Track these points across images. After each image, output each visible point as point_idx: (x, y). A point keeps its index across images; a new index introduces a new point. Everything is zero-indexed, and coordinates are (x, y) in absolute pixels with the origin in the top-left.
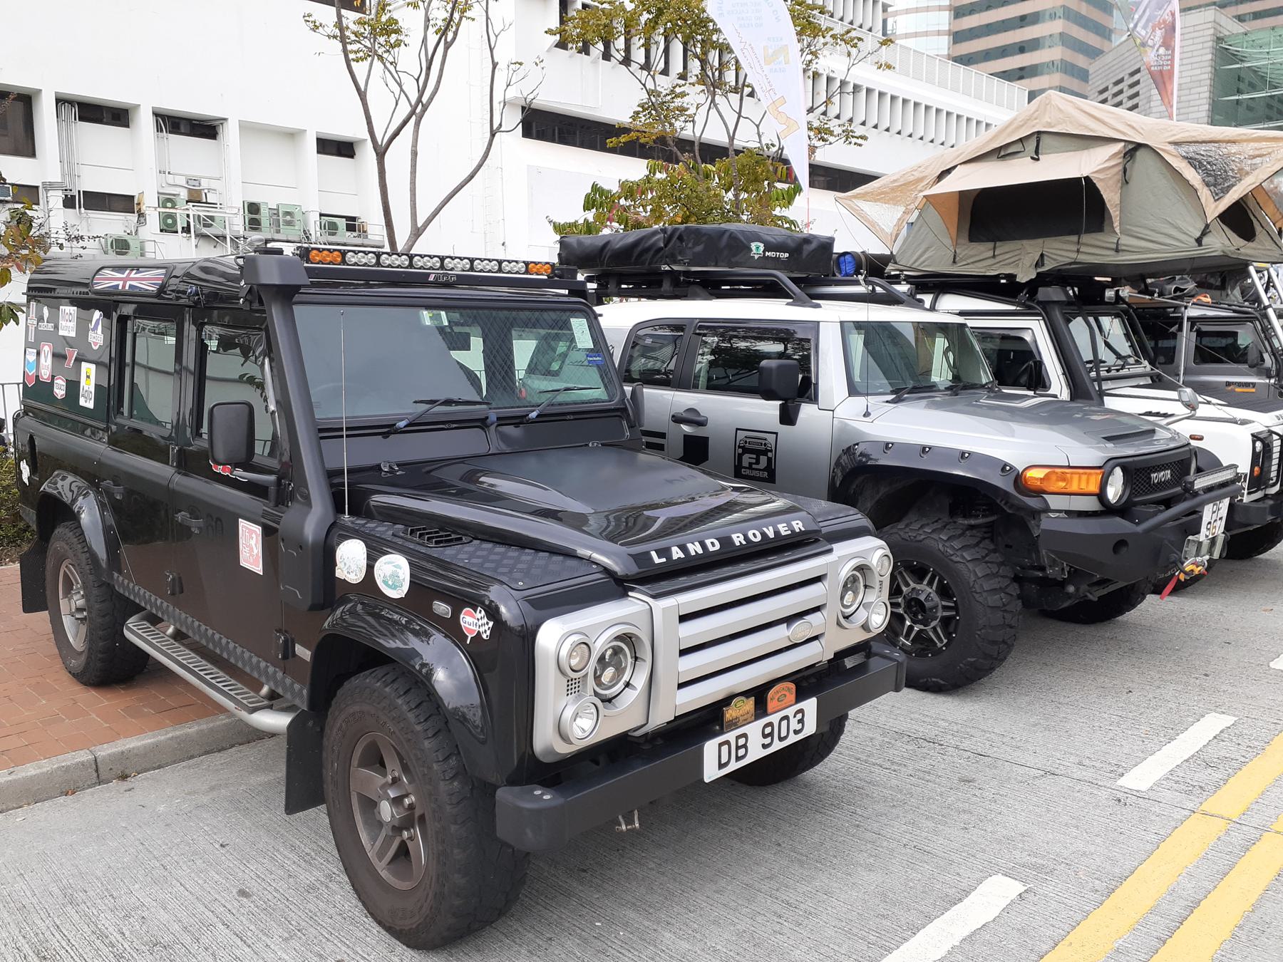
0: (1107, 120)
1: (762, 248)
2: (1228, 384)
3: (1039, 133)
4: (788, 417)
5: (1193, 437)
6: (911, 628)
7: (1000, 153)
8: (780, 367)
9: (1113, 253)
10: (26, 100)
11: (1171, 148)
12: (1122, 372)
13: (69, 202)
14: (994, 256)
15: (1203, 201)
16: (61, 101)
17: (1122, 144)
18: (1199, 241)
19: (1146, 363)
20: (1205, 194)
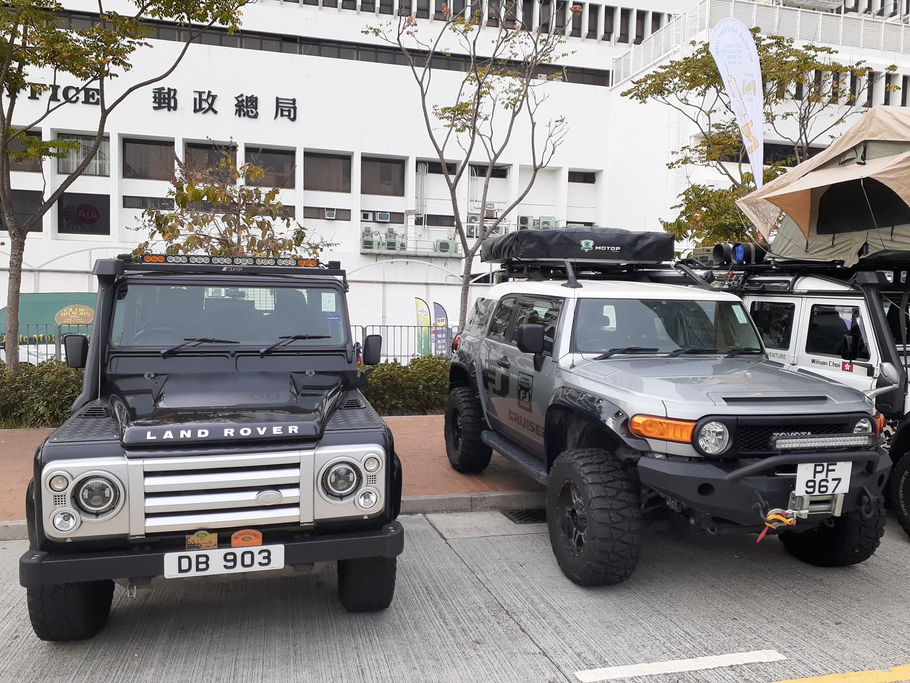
1: (591, 243)
3: (866, 142)
7: (840, 160)
10: (401, 163)
13: (418, 222)
14: (833, 246)
16: (419, 162)
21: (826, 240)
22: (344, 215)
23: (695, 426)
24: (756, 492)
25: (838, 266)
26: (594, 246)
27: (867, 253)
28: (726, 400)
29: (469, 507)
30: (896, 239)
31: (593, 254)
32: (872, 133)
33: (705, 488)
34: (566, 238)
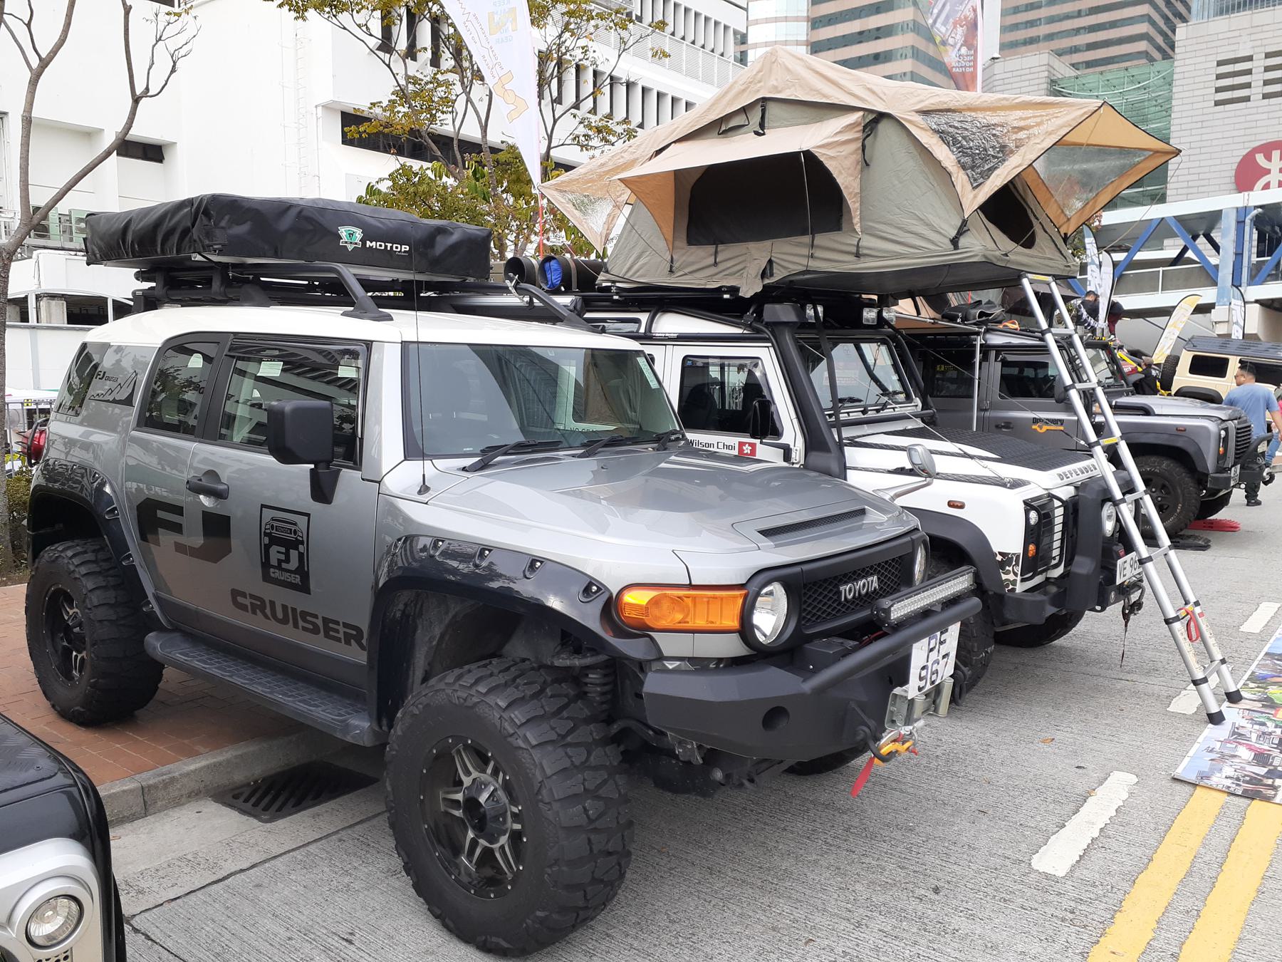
0: (842, 82)
1: (358, 234)
2: (1036, 421)
3: (764, 100)
4: (322, 490)
5: (951, 504)
6: (474, 843)
7: (720, 127)
8: (297, 411)
9: (852, 258)
11: (918, 118)
12: (883, 414)
14: (716, 264)
15: (959, 188)
17: (861, 113)
18: (955, 242)
19: (918, 401)
20: (961, 179)
21: (702, 254)
23: (746, 596)
24: (853, 705)
25: (726, 296)
26: (363, 241)
27: (772, 275)
30: (818, 253)
31: (362, 257)
32: (776, 87)
33: (774, 715)
34: (309, 220)
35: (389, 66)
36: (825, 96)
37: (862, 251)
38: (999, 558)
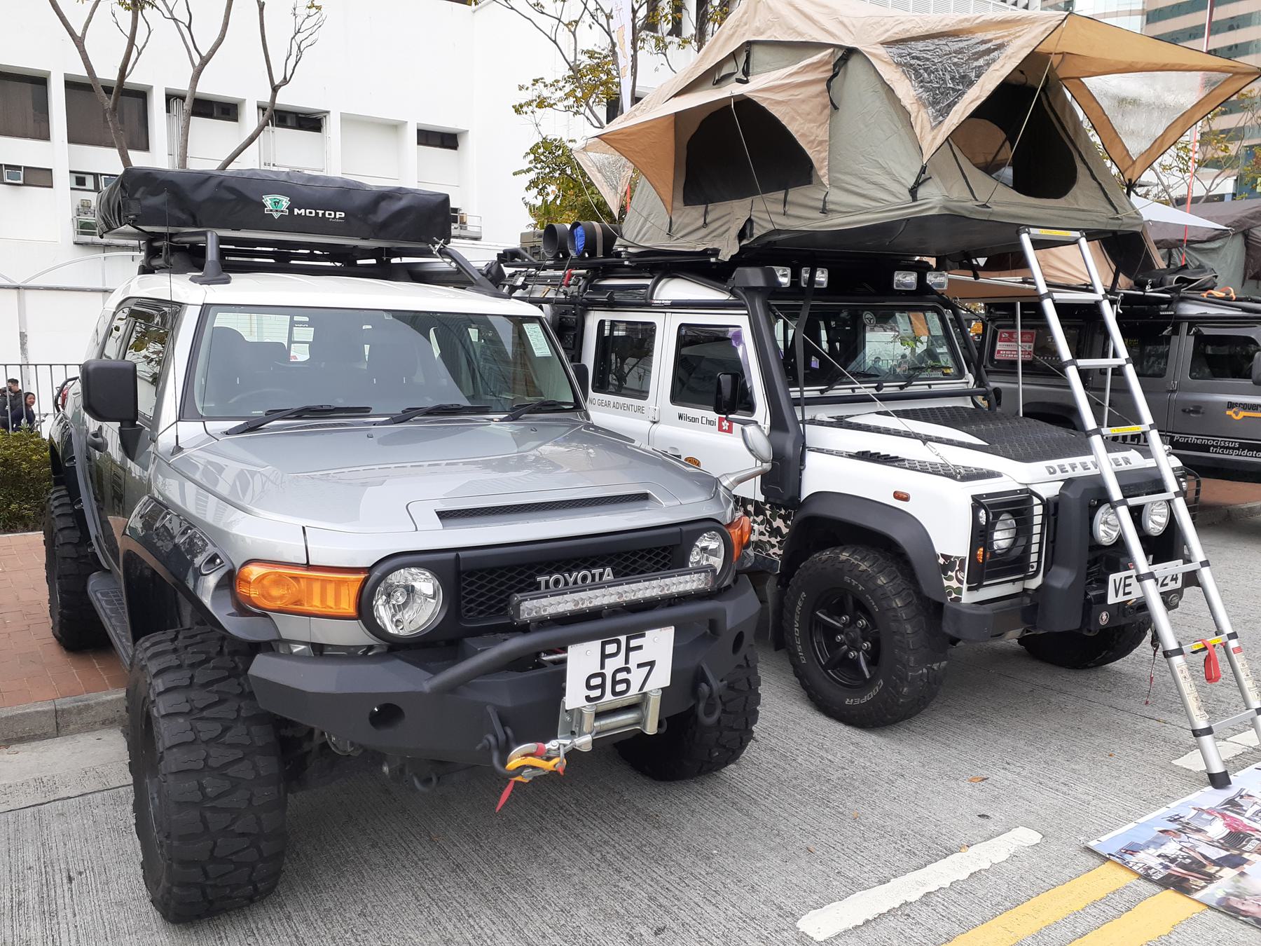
0: (817, 17)
1: (285, 202)
2: (1231, 405)
3: (749, 44)
5: (898, 496)
9: (818, 215)
11: (882, 51)
12: (910, 389)
14: (705, 224)
15: (917, 130)
17: (830, 50)
19: (970, 378)
20: (922, 118)
21: (694, 214)
22: (39, 177)
23: (366, 581)
24: (490, 709)
25: (713, 260)
26: (290, 209)
27: (752, 236)
28: (443, 515)
29: (51, 729)
30: (792, 210)
31: (289, 222)
32: (758, 29)
33: (388, 713)
34: (232, 190)
35: (555, 42)
36: (800, 34)
37: (830, 207)
38: (941, 561)
